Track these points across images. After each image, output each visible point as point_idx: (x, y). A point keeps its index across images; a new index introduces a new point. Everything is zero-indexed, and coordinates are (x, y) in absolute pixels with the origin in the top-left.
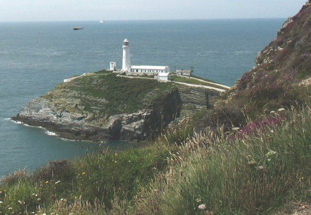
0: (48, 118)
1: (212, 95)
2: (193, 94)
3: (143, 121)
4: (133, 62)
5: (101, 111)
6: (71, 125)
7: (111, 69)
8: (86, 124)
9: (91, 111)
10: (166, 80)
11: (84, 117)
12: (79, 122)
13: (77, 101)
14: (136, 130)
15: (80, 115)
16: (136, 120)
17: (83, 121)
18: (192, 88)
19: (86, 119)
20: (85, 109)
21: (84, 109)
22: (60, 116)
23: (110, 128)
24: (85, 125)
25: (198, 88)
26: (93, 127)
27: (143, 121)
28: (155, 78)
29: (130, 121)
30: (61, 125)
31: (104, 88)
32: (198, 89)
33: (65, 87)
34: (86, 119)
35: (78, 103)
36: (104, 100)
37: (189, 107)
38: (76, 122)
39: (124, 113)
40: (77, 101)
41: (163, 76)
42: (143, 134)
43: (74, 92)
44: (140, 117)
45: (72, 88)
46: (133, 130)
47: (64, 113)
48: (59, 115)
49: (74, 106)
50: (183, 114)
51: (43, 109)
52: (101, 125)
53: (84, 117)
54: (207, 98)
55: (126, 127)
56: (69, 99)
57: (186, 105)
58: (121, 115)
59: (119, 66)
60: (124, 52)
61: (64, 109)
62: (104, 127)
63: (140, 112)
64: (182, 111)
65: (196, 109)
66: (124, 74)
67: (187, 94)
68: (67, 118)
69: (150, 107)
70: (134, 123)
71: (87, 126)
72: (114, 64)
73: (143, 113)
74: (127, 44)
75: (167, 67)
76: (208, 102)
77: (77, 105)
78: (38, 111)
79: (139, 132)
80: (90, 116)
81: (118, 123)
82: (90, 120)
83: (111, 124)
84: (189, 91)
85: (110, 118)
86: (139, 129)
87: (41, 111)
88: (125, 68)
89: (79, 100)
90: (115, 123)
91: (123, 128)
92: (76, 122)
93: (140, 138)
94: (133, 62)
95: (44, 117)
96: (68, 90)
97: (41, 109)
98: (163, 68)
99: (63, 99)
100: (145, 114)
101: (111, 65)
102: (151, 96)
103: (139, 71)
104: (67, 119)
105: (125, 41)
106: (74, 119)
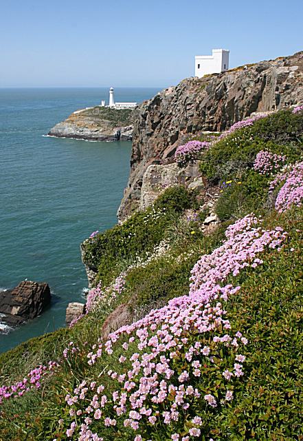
9: (102, 127)
12: (96, 133)
13: (92, 122)
16: (128, 130)
29: (125, 130)
40: (92, 122)
60: (111, 95)
61: (85, 127)
68: (87, 132)
74: (112, 90)
81: (119, 132)
82: (102, 131)
83: (116, 133)
88: (111, 104)
105: (112, 88)
106: (92, 132)
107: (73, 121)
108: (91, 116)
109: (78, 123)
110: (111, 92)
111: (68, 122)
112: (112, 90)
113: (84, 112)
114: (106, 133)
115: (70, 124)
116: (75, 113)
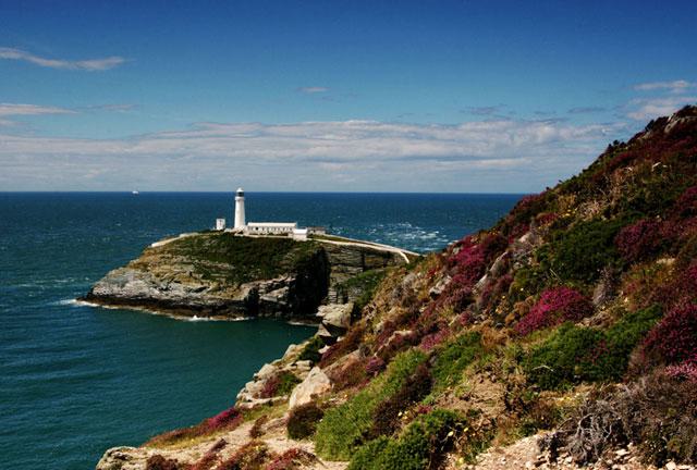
0: (142, 295)
3: (287, 288)
5: (228, 279)
7: (219, 227)
8: (209, 296)
9: (213, 280)
10: (304, 238)
11: (205, 288)
12: (199, 295)
14: (279, 299)
15: (199, 286)
16: (277, 287)
17: (204, 292)
18: (342, 247)
20: (203, 278)
21: (203, 278)
22: (167, 289)
23: (245, 299)
24: (208, 298)
25: (351, 246)
27: (287, 288)
28: (290, 236)
29: (270, 289)
30: (170, 301)
31: (222, 251)
32: (351, 248)
33: (162, 252)
36: (227, 265)
38: (195, 295)
39: (259, 279)
40: (191, 268)
43: (180, 258)
44: (283, 284)
45: (175, 253)
46: (275, 300)
47: (173, 285)
49: (188, 274)
53: (205, 288)
54: (363, 259)
55: (265, 297)
56: (176, 266)
57: (335, 268)
58: (257, 283)
59: (230, 223)
60: (238, 205)
61: (172, 279)
62: (236, 298)
63: (283, 278)
64: (331, 275)
66: (241, 233)
68: (178, 291)
69: (293, 271)
70: (275, 291)
71: (211, 299)
72: (224, 221)
76: (363, 262)
78: (123, 286)
79: (284, 303)
80: (213, 286)
81: (254, 293)
84: (338, 250)
85: (243, 286)
86: (283, 299)
87: (128, 285)
88: (239, 225)
89: (192, 266)
92: (195, 295)
93: (284, 309)
94: (248, 219)
95: (136, 292)
96: (170, 255)
97: (127, 282)
98: (293, 225)
99: (167, 267)
100: (289, 280)
101: (218, 222)
102: (290, 257)
103: (260, 230)
104: (177, 293)
105: (239, 190)
106: (190, 290)
107: (145, 265)
108: (189, 253)
109: (157, 270)
110: (237, 198)
111: (136, 267)
113: (174, 242)
114: (222, 296)
115: (139, 272)
116: (154, 245)
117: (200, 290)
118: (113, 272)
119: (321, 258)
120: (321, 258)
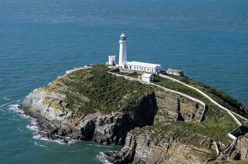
1: (184, 102)
2: (167, 100)
4: (130, 58)
6: (53, 121)
8: (65, 121)
15: (61, 113)
19: (66, 116)
23: (82, 129)
24: (64, 122)
26: (69, 125)
27: (113, 124)
34: (66, 116)
35: (63, 99)
36: (86, 99)
37: (162, 113)
41: (146, 79)
42: (112, 138)
48: (47, 109)
50: (157, 119)
51: (41, 100)
52: (76, 125)
64: (156, 116)
65: (168, 115)
67: (162, 98)
71: (65, 124)
73: (116, 116)
74: (124, 39)
75: (159, 65)
77: (61, 102)
83: (82, 125)
89: (64, 96)
90: (88, 123)
91: (96, 129)
100: (116, 118)
101: (109, 58)
105: (123, 35)
112: (124, 39)
116: (67, 72)
117: (61, 115)
118: (36, 90)
119: (150, 100)
120: (150, 100)
